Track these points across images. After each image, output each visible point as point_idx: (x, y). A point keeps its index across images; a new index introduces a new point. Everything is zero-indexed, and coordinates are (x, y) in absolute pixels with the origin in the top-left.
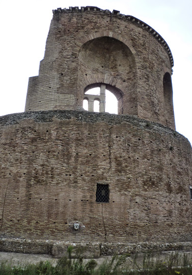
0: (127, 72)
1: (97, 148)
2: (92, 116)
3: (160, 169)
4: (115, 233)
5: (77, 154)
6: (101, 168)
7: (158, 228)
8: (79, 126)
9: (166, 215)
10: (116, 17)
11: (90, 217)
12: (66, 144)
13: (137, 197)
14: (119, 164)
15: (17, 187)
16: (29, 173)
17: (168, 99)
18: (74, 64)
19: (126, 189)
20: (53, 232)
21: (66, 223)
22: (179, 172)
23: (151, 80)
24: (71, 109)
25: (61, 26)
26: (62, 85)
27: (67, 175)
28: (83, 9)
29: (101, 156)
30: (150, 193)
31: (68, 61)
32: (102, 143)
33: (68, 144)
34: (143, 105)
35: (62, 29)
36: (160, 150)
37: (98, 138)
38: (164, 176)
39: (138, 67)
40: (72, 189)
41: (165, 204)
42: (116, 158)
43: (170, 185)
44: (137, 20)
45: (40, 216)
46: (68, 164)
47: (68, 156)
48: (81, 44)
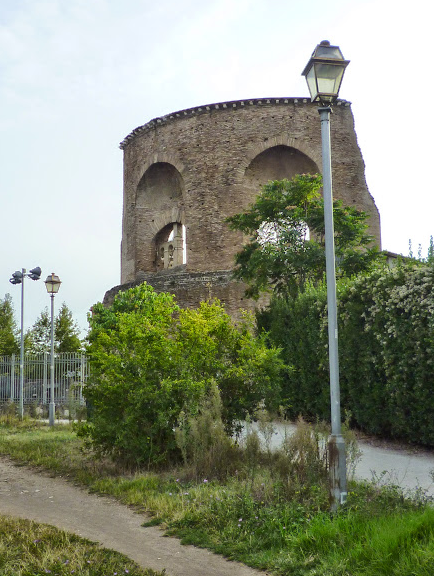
10: (160, 125)
23: (207, 199)
44: (181, 113)
48: (135, 188)
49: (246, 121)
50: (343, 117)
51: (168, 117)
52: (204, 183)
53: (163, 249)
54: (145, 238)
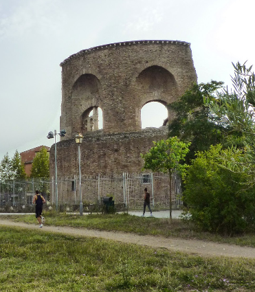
3: (105, 167)
50: (186, 52)
51: (92, 49)
52: (113, 86)
53: (87, 121)
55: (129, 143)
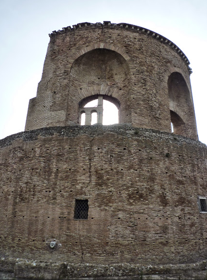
0: (123, 79)
1: (77, 162)
2: (75, 130)
3: (152, 179)
4: (93, 252)
5: (57, 170)
6: (80, 183)
7: (147, 246)
8: (60, 141)
9: (158, 232)
11: (67, 235)
12: (48, 160)
13: (120, 212)
14: (100, 177)
15: (6, 205)
16: (15, 192)
17: (185, 100)
18: (66, 81)
19: (107, 204)
20: (32, 250)
21: (44, 241)
22: (179, 181)
23: (149, 84)
24: (62, 125)
25: (56, 48)
26: (54, 103)
27: (47, 192)
28: (75, 27)
29: (81, 170)
30: (137, 207)
31: (60, 79)
32: (82, 156)
33: (49, 160)
34: (138, 111)
35: (56, 50)
36: (151, 158)
37: (78, 152)
38: (157, 187)
39: (132, 73)
40: (51, 206)
41: (157, 219)
42: (96, 172)
43: (165, 197)
44: (130, 26)
45: (22, 233)
46: (48, 180)
47: (48, 171)
48: (72, 61)
49: (166, 50)
54: (74, 98)
55: (181, 147)
